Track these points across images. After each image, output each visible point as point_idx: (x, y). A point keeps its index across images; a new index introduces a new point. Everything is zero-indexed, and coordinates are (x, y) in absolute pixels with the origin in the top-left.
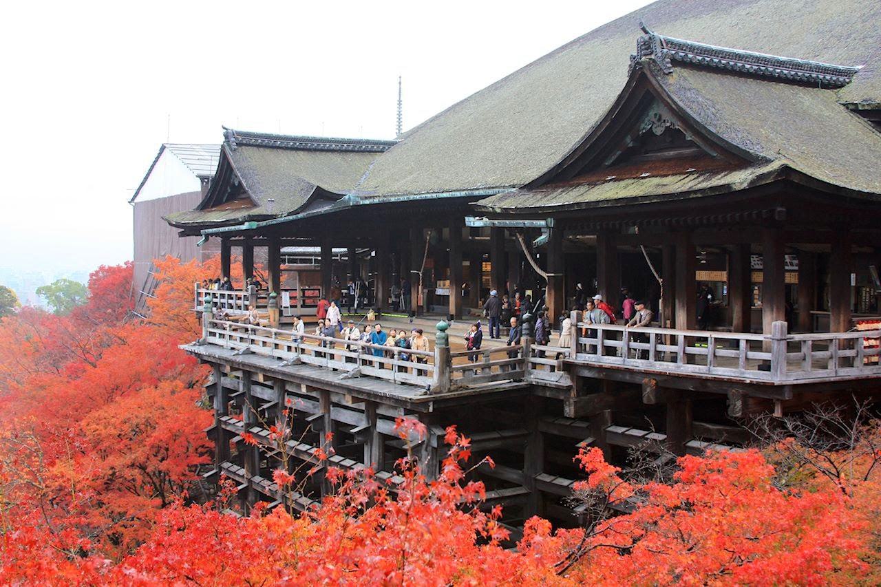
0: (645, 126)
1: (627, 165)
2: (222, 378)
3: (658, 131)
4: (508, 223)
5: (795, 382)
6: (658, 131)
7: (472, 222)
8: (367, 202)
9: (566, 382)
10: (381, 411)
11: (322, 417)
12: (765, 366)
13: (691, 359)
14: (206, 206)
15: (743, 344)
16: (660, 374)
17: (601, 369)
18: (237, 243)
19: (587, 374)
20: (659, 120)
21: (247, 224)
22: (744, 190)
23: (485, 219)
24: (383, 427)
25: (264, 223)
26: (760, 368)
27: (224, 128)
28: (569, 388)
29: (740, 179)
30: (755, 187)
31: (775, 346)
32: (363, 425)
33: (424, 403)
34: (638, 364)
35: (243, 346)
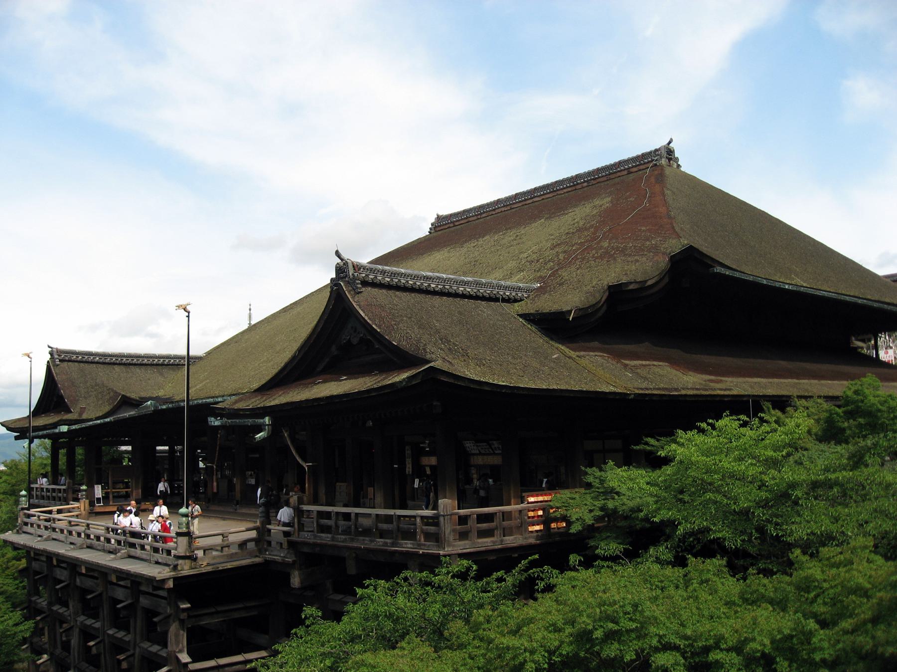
1: (334, 370)
2: (33, 563)
3: (355, 341)
5: (460, 552)
6: (355, 341)
7: (215, 422)
10: (143, 588)
11: (100, 595)
17: (315, 545)
19: (306, 550)
20: (355, 331)
23: (225, 420)
24: (144, 601)
25: (74, 427)
32: (129, 601)
33: (164, 581)
34: (342, 540)
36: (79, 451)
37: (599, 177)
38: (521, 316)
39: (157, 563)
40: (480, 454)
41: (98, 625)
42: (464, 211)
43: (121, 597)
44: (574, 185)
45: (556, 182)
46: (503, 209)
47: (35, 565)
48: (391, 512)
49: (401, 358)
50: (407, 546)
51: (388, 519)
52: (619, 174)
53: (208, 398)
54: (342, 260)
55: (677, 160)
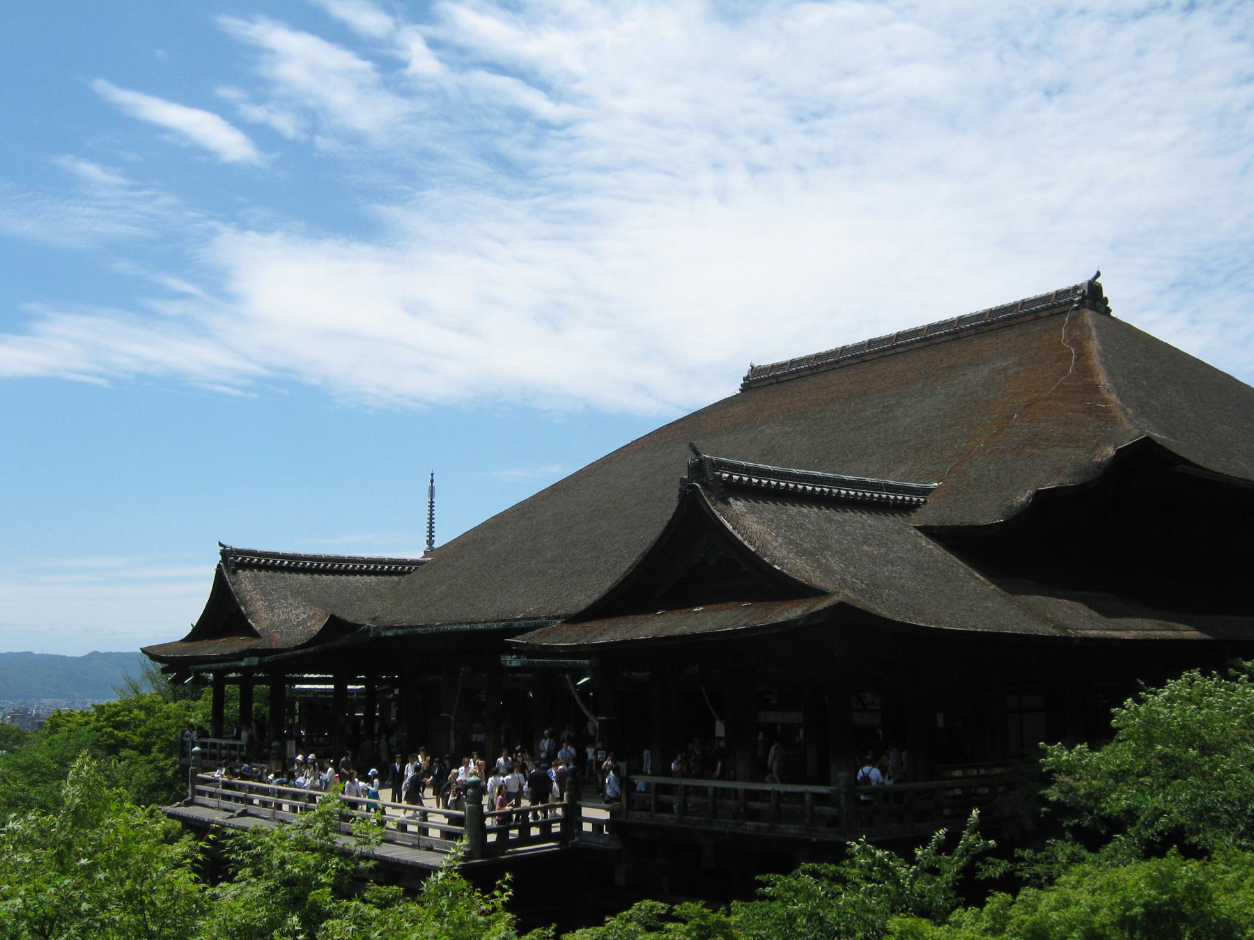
1: (680, 600)
7: (512, 661)
8: (390, 634)
9: (616, 845)
12: (833, 822)
13: (754, 815)
15: (808, 798)
18: (233, 681)
21: (246, 660)
25: (266, 659)
26: (830, 825)
27: (221, 545)
31: (843, 801)
35: (240, 807)
37: (993, 322)
38: (918, 528)
39: (430, 849)
42: (793, 362)
44: (956, 332)
45: (930, 326)
46: (850, 362)
48: (768, 787)
49: (792, 589)
50: (791, 830)
52: (1022, 319)
53: (461, 624)
55: (1106, 300)
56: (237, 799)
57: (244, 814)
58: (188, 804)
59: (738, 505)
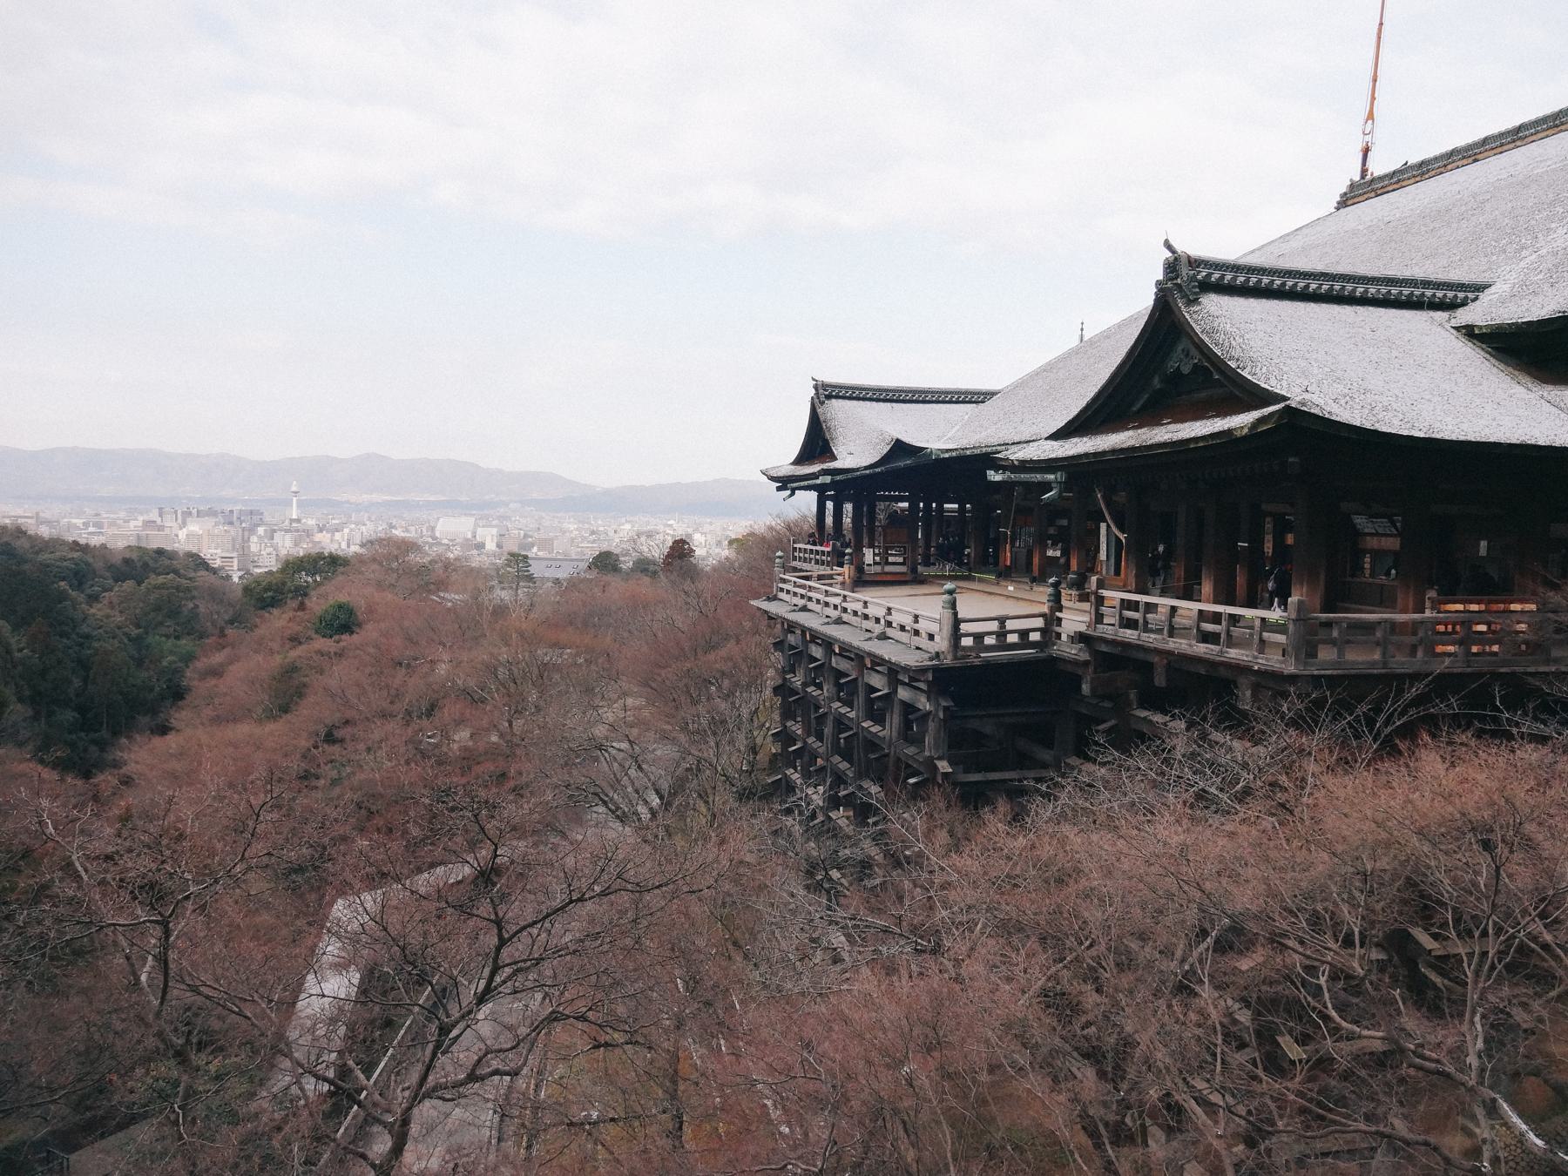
0: (1172, 365)
3: (1186, 370)
4: (1024, 477)
6: (1186, 370)
7: (994, 476)
9: (1085, 656)
13: (1206, 638)
14: (800, 460)
16: (1170, 653)
17: (1114, 643)
19: (1104, 648)
22: (1244, 438)
24: (903, 694)
28: (1086, 663)
29: (1240, 421)
30: (1255, 434)
31: (1291, 627)
34: (1150, 639)
36: (848, 507)
40: (1377, 534)
41: (852, 715)
43: (878, 686)
47: (791, 639)
51: (1216, 619)
54: (1173, 251)
56: (802, 596)
57: (804, 609)
58: (769, 599)
59: (1213, 304)
